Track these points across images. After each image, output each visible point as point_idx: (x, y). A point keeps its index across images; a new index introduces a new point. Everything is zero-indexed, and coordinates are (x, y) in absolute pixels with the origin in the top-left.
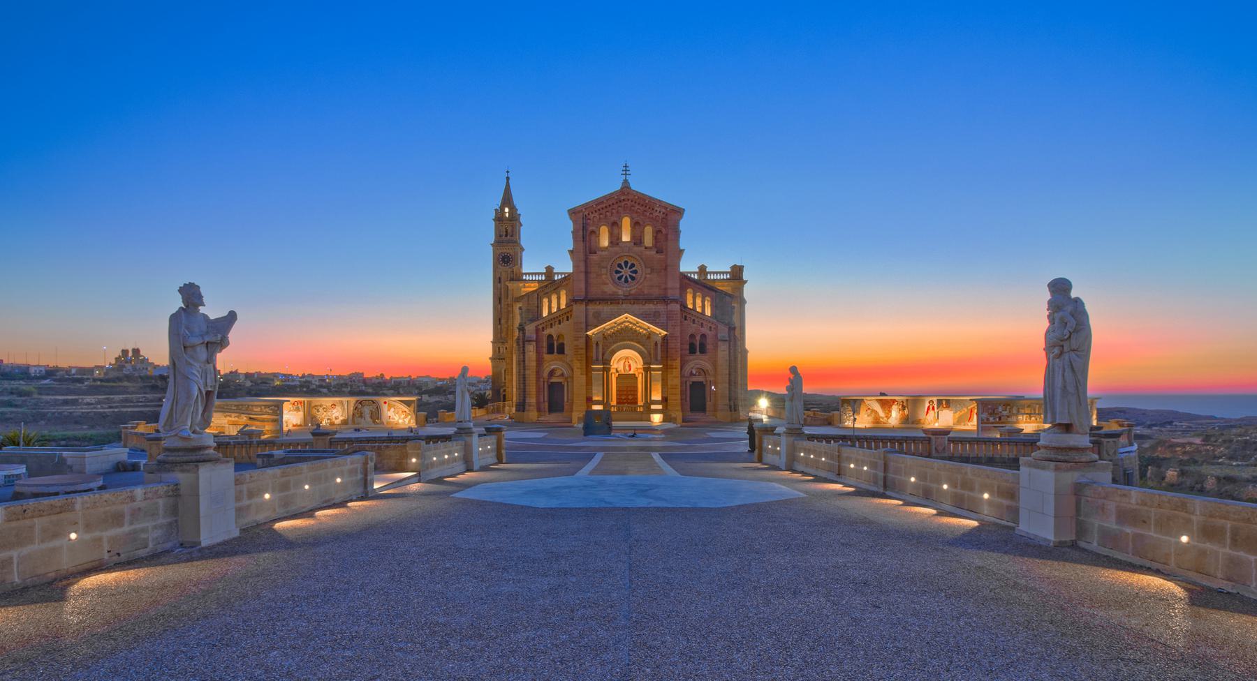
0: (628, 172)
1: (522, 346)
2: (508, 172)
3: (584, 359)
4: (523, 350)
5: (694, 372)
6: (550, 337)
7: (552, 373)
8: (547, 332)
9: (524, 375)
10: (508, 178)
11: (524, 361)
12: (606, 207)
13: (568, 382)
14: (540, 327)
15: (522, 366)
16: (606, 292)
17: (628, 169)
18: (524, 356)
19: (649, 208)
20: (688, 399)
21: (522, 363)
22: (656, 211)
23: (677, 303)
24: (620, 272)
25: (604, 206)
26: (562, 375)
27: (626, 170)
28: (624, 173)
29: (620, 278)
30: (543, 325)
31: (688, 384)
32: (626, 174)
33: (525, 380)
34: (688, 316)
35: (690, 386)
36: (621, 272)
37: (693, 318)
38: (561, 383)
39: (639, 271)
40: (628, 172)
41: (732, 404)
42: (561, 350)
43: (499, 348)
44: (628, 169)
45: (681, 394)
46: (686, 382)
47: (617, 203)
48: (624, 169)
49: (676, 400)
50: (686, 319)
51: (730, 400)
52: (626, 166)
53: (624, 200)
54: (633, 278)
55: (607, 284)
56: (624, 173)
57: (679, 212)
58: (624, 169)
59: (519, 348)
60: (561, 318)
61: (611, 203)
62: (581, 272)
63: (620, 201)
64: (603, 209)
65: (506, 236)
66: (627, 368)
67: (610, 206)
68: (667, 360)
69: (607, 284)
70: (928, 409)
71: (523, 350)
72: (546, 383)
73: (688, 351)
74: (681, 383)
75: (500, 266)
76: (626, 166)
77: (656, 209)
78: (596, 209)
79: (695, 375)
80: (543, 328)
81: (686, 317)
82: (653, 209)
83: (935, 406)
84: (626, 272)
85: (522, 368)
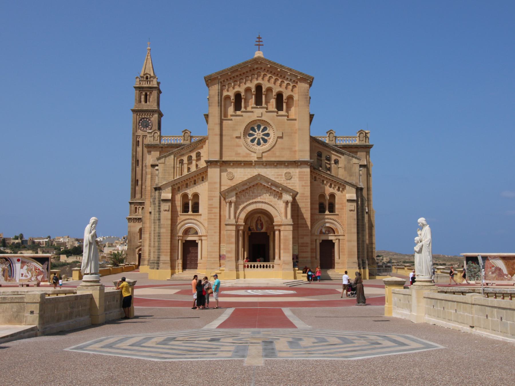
0: (261, 43)
1: (157, 204)
5: (324, 231)
6: (185, 196)
7: (187, 232)
9: (159, 233)
11: (159, 220)
12: (240, 75)
13: (202, 240)
14: (176, 187)
15: (157, 224)
16: (239, 154)
17: (261, 40)
18: (159, 214)
19: (281, 76)
20: (318, 257)
21: (157, 221)
22: (287, 78)
23: (307, 165)
25: (237, 73)
26: (196, 233)
28: (258, 43)
29: (252, 141)
30: (179, 185)
31: (318, 242)
33: (160, 239)
34: (318, 177)
35: (320, 244)
36: (254, 135)
37: (322, 179)
38: (195, 241)
39: (272, 135)
40: (261, 43)
41: (361, 262)
42: (196, 209)
44: (261, 40)
45: (312, 252)
46: (316, 240)
47: (250, 71)
48: (258, 40)
49: (307, 257)
50: (315, 180)
51: (358, 258)
52: (259, 38)
53: (257, 68)
55: (241, 146)
56: (258, 43)
58: (258, 40)
59: (155, 207)
60: (196, 179)
61: (245, 71)
62: (216, 135)
63: (254, 70)
64: (237, 76)
65: (146, 102)
66: (259, 227)
67: (244, 73)
68: (298, 219)
69: (241, 146)
71: (159, 209)
72: (180, 241)
73: (318, 211)
74: (312, 241)
75: (139, 130)
76: (259, 38)
77: (287, 77)
78: (231, 77)
79: (325, 233)
80: (179, 188)
81: (315, 177)
82: (284, 77)
84: (258, 134)
85: (157, 226)
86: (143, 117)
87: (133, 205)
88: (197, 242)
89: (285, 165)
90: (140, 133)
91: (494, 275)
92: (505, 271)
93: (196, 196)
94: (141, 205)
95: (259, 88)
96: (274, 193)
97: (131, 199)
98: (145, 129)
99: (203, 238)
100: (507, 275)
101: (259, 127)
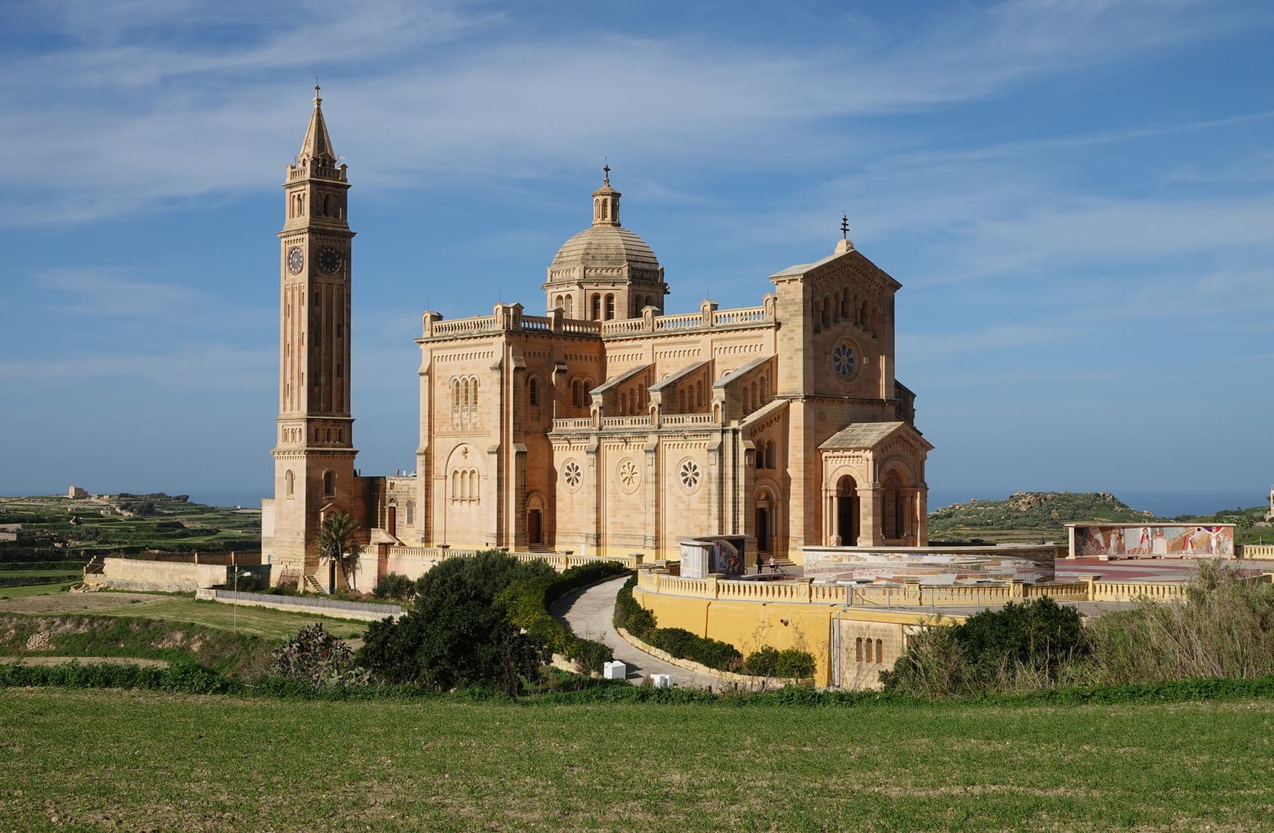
0: (847, 227)
2: (318, 88)
3: (813, 476)
4: (734, 462)
8: (760, 435)
10: (319, 100)
13: (776, 508)
17: (847, 222)
24: (839, 360)
26: (768, 498)
27: (845, 225)
28: (843, 227)
30: (756, 427)
32: (845, 230)
40: (847, 227)
43: (317, 430)
44: (847, 222)
54: (850, 369)
57: (897, 286)
58: (843, 222)
70: (1143, 537)
75: (319, 272)
76: (845, 220)
77: (876, 280)
83: (1150, 535)
84: (844, 360)
86: (325, 244)
87: (312, 424)
88: (767, 510)
89: (872, 405)
90: (322, 279)
91: (1093, 549)
92: (1102, 545)
93: (769, 443)
94: (324, 425)
95: (846, 290)
96: (909, 448)
97: (308, 411)
98: (329, 270)
99: (780, 505)
100: (1103, 548)
101: (844, 347)
